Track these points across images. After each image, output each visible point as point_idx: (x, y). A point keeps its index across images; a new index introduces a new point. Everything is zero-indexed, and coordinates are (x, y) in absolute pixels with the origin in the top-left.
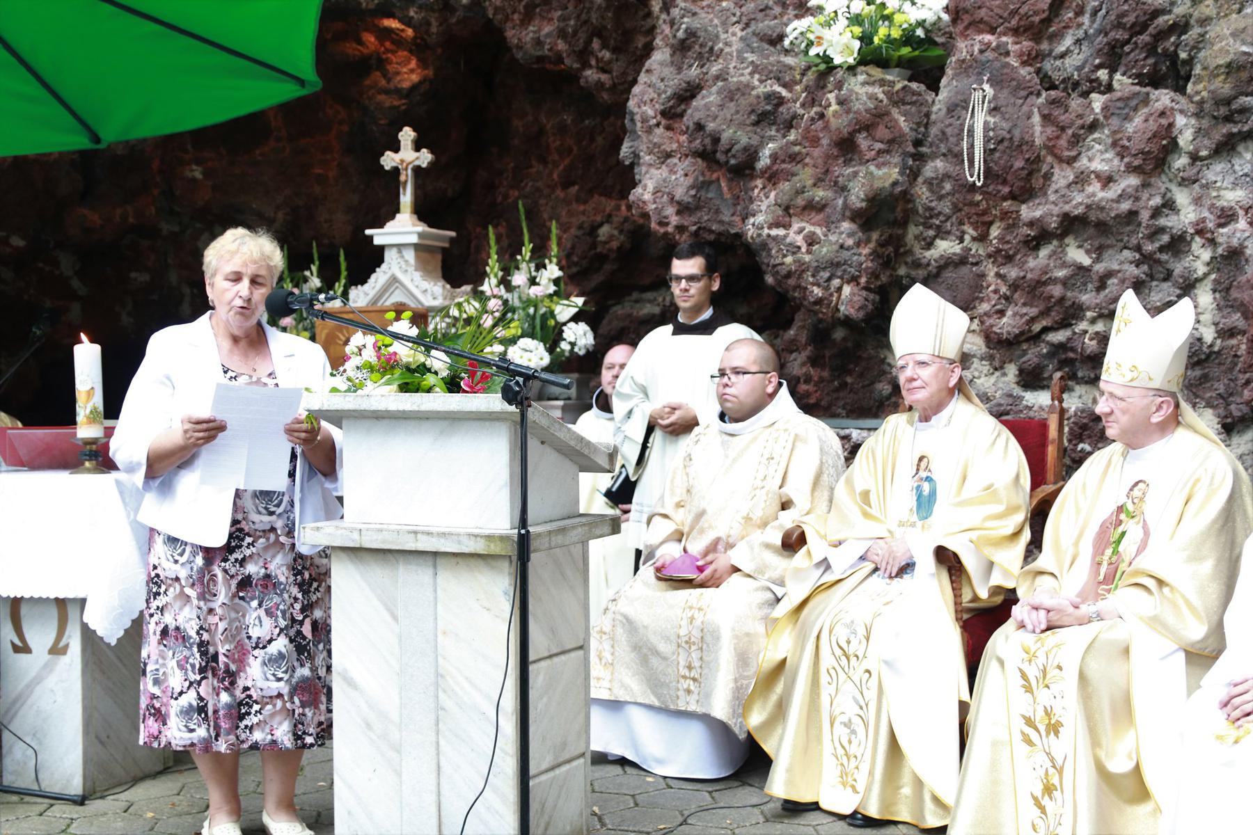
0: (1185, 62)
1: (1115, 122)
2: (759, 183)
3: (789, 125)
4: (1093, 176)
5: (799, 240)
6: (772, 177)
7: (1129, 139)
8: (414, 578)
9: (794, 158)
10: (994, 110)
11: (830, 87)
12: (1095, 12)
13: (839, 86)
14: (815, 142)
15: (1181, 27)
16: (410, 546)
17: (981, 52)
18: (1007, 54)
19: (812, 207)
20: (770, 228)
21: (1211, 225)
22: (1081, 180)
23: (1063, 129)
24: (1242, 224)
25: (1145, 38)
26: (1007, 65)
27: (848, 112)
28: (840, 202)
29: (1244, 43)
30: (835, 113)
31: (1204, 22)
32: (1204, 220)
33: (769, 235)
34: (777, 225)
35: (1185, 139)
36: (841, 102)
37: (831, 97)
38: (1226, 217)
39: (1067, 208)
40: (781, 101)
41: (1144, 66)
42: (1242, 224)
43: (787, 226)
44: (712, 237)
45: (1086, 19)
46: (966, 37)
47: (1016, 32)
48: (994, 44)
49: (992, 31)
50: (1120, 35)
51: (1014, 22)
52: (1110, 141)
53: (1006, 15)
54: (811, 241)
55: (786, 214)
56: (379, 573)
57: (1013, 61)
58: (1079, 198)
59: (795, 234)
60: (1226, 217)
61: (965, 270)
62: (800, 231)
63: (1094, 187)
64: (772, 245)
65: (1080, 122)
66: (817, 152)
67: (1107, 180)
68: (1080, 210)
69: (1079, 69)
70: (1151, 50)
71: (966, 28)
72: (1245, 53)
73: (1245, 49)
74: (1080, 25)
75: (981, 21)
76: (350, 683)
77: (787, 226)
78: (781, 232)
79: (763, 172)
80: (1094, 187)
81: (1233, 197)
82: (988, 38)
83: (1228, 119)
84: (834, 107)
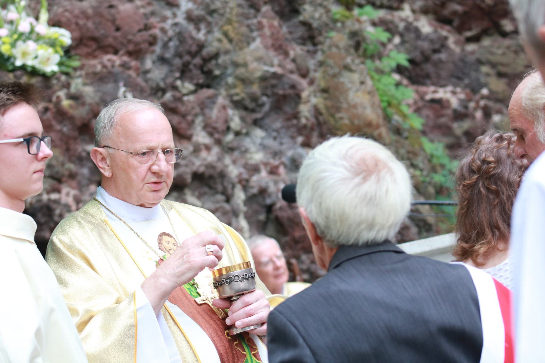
0: (216, 77)
1: (207, 111)
4: (203, 147)
7: (216, 122)
11: (56, 88)
12: (165, 46)
13: (67, 86)
15: (216, 56)
17: (113, 66)
18: (129, 68)
19: (72, 176)
20: (48, 192)
21: (245, 176)
22: (197, 150)
23: (184, 116)
24: (264, 173)
25: (197, 61)
26: (130, 76)
27: (83, 104)
28: (85, 171)
29: (265, 64)
30: (71, 106)
31: (227, 52)
32: (240, 174)
33: (49, 200)
35: (236, 123)
36: (71, 97)
37: (62, 94)
38: (255, 169)
39: (194, 168)
41: (199, 79)
42: (264, 173)
43: (59, 191)
45: (158, 49)
46: (95, 57)
47: (130, 54)
48: (118, 62)
49: (116, 52)
50: (187, 58)
51: (131, 47)
52: (202, 124)
53: (125, 41)
57: (132, 73)
58: (197, 163)
60: (255, 169)
62: (68, 194)
63: (204, 154)
64: (54, 206)
65: (194, 112)
67: (208, 148)
68: (202, 169)
69: (164, 79)
70: (201, 68)
71: (94, 51)
72: (267, 72)
73: (266, 68)
74: (153, 52)
75: (110, 46)
77: (59, 191)
78: (54, 196)
80: (204, 154)
81: (257, 157)
82: (114, 58)
83: (253, 111)
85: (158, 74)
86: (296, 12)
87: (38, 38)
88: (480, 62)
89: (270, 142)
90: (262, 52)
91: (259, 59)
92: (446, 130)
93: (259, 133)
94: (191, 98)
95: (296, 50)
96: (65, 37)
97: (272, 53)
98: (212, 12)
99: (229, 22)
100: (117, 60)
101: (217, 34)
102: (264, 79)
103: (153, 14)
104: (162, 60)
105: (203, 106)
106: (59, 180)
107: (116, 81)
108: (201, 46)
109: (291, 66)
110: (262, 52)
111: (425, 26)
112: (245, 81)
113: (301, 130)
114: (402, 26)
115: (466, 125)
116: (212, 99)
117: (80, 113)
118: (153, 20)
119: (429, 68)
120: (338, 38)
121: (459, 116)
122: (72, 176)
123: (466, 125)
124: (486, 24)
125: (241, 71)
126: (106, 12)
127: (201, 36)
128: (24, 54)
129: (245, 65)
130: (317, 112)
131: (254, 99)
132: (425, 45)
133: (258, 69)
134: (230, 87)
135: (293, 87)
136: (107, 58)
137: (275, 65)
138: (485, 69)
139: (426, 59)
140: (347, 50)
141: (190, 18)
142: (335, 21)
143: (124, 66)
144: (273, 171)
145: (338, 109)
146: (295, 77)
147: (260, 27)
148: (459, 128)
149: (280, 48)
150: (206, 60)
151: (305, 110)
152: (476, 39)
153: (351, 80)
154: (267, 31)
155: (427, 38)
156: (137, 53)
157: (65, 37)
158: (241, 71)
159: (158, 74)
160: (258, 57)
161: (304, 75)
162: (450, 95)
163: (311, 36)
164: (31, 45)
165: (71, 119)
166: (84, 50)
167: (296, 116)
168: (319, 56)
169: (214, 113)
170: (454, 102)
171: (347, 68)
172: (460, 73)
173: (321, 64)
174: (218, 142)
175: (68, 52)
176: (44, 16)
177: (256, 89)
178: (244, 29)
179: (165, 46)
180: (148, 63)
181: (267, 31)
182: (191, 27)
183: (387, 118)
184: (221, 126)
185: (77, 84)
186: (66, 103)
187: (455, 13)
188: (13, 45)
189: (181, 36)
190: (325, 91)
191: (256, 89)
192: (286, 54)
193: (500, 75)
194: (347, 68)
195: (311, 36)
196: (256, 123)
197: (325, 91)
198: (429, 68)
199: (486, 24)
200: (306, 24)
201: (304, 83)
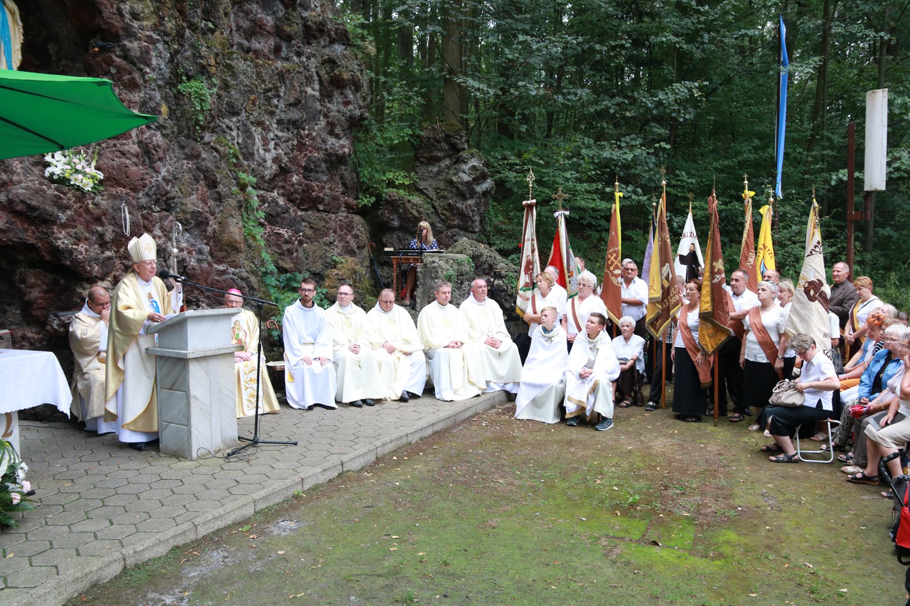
2: (55, 227)
3: (67, 207)
5: (83, 250)
6: (64, 226)
8: (213, 363)
9: (74, 221)
10: (130, 213)
12: (150, 189)
13: (94, 199)
14: (80, 215)
15: (174, 198)
16: (219, 353)
19: (86, 239)
23: (151, 222)
25: (164, 198)
34: (75, 244)
36: (94, 204)
40: (61, 198)
44: (10, 243)
45: (146, 189)
47: (131, 189)
54: (87, 251)
55: (78, 240)
56: (204, 364)
59: (82, 247)
61: (111, 261)
66: (81, 219)
67: (160, 237)
76: (196, 398)
79: (61, 224)
81: (184, 245)
84: (91, 206)
85: (144, 201)
86: (216, 187)
87: (85, 174)
88: (304, 220)
89: (191, 240)
90: (195, 201)
91: (193, 204)
92: (280, 247)
93: (188, 235)
94: (157, 214)
95: (212, 203)
96: (101, 176)
97: (200, 202)
98: (176, 179)
99: (183, 185)
100: (124, 191)
101: (177, 189)
102: (193, 212)
103: (147, 174)
104: (147, 195)
105: (161, 219)
106: (79, 241)
107: (122, 200)
108: (167, 193)
109: (207, 209)
110: (195, 201)
111: (281, 201)
112: (184, 212)
113: (206, 237)
114: (270, 199)
115: (289, 246)
116: (167, 217)
117: (97, 212)
118: (146, 176)
119: (279, 219)
120: (232, 202)
121: (287, 242)
122: (86, 239)
123: (289, 246)
124: (311, 205)
125: (183, 207)
126: (123, 169)
127: (168, 188)
128: (76, 179)
129: (186, 205)
130: (215, 232)
131: (187, 220)
132: (279, 209)
133: (191, 208)
134: (177, 213)
135: (206, 218)
136: (119, 189)
137: (200, 207)
138: (303, 224)
139: (278, 215)
140: (234, 208)
141: (164, 179)
142: (232, 194)
143: (127, 194)
144: (190, 252)
145: (224, 232)
146: (208, 214)
147: (197, 190)
148: (286, 247)
149: (204, 201)
150: (168, 199)
151: (209, 229)
152: (306, 210)
153: (232, 221)
154: (200, 192)
155: (281, 206)
156: (135, 190)
157: (101, 176)
158: (183, 207)
159: (144, 201)
160: (193, 203)
161: (212, 215)
162: (285, 233)
163: (219, 198)
164: (80, 176)
165: (92, 213)
166: (109, 183)
167: (205, 231)
168: (221, 208)
169: (166, 223)
170: (286, 236)
171: (232, 216)
172: (292, 224)
173: (221, 211)
174: (166, 236)
175: (101, 182)
176: (94, 164)
177: (188, 216)
178: (189, 189)
179: (150, 189)
180: (140, 195)
181: (200, 192)
182: (164, 184)
183: (246, 240)
184: (168, 229)
185: (98, 199)
186: (91, 206)
187: (297, 199)
188: (71, 175)
189: (158, 186)
190: (220, 223)
191: (188, 216)
192: (206, 204)
193: (311, 228)
194: (232, 216)
195: (219, 198)
196: (186, 230)
197: (220, 223)
198: (279, 219)
199: (311, 205)
200: (217, 192)
201: (212, 218)
